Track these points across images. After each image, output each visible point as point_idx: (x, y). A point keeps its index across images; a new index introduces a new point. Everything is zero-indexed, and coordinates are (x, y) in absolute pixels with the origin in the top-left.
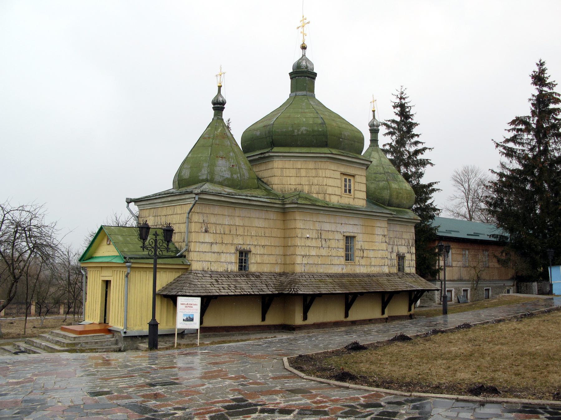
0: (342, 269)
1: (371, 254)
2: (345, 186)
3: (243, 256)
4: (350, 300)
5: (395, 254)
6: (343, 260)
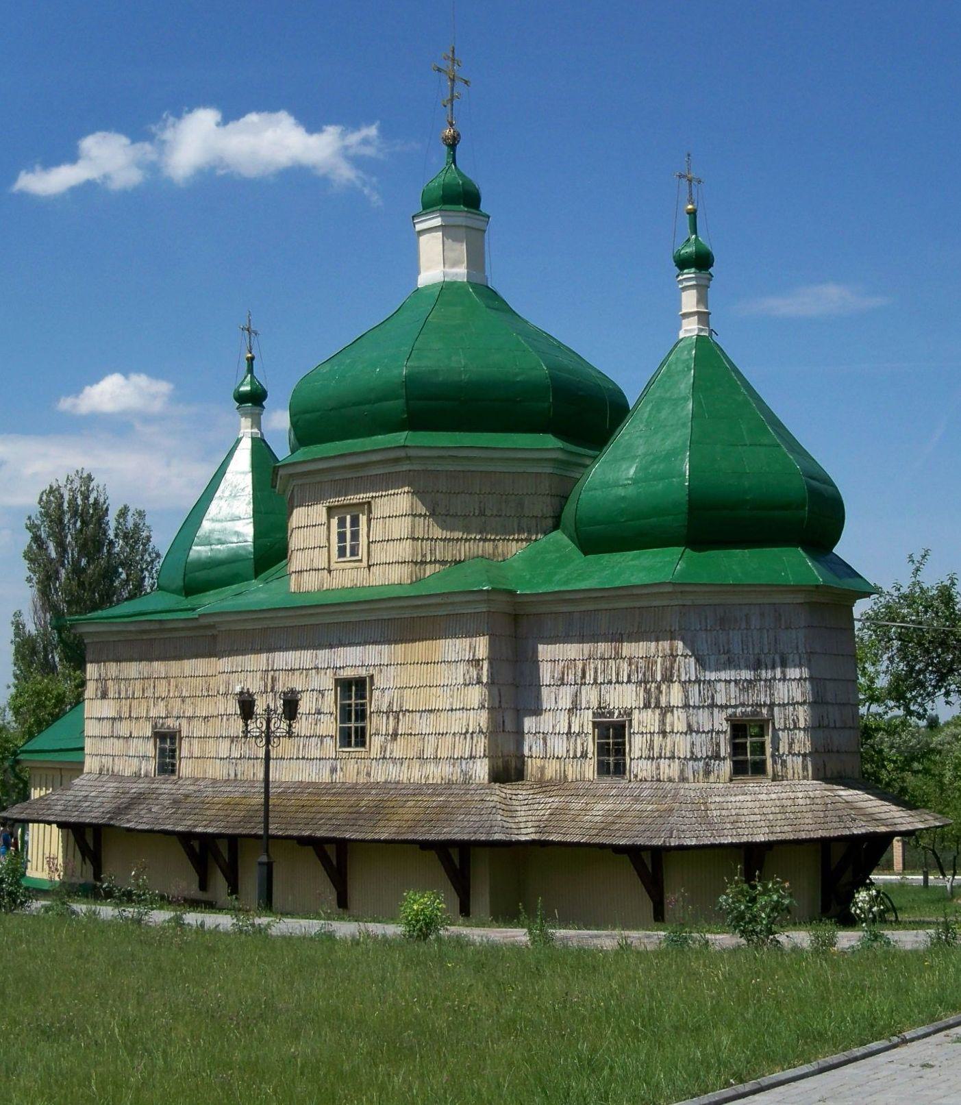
0: (333, 770)
1: (424, 725)
2: (342, 537)
3: (167, 742)
4: (457, 861)
5: (588, 716)
6: (330, 748)
